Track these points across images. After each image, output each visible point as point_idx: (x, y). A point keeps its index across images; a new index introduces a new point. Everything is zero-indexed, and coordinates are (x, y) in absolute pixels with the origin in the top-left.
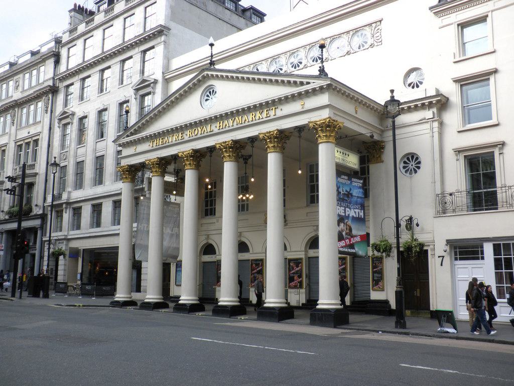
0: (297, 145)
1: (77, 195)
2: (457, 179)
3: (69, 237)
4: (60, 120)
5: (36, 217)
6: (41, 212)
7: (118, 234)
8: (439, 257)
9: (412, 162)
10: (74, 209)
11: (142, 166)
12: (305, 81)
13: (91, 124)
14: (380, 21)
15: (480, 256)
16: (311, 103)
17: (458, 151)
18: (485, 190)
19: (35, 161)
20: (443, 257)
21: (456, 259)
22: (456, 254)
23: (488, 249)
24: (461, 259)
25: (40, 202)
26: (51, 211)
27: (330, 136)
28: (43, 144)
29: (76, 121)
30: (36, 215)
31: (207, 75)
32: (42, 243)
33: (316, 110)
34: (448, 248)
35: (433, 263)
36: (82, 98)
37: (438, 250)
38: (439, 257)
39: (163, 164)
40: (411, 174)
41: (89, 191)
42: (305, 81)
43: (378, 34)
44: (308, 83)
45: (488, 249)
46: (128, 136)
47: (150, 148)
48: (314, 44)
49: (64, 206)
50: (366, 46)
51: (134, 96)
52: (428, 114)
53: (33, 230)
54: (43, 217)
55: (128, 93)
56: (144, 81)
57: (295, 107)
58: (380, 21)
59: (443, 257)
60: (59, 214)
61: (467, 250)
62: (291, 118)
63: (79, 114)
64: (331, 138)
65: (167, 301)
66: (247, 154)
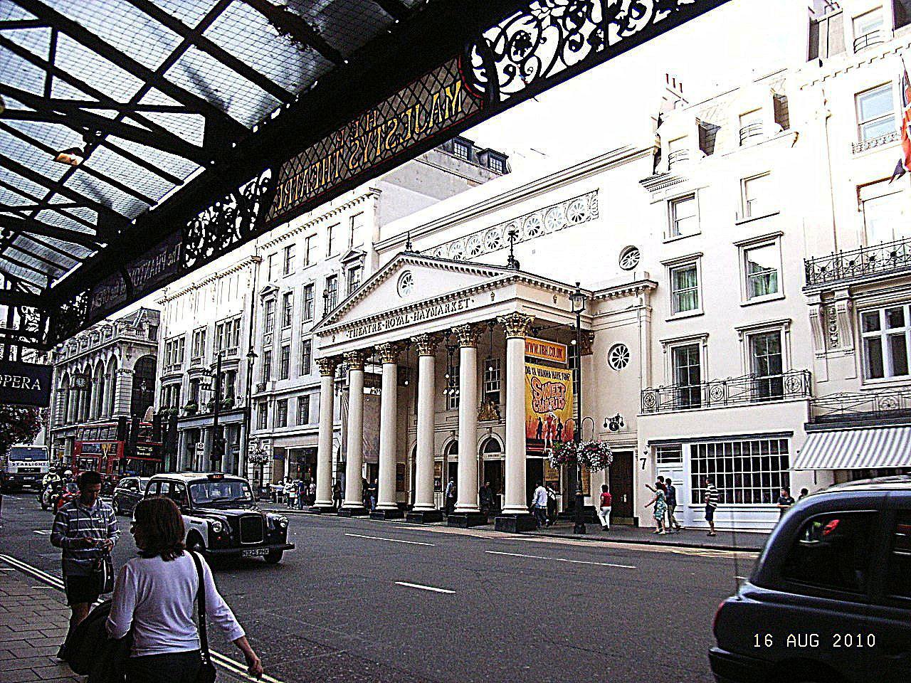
0: (488, 339)
1: (282, 385)
2: (664, 374)
3: (274, 435)
4: (263, 296)
5: (239, 411)
6: (244, 405)
7: (317, 434)
8: (641, 459)
9: (620, 354)
10: (280, 402)
11: (339, 359)
12: (494, 271)
13: (297, 301)
14: (597, 191)
15: (661, 459)
16: (501, 294)
17: (666, 343)
18: (773, 377)
19: (237, 345)
20: (645, 459)
21: (659, 462)
22: (659, 457)
23: (686, 449)
24: (664, 461)
25: (243, 394)
26: (255, 404)
27: (518, 331)
28: (245, 325)
29: (280, 297)
30: (238, 409)
31: (403, 259)
32: (247, 441)
33: (505, 303)
34: (649, 450)
35: (637, 464)
36: (287, 270)
37: (642, 450)
38: (641, 459)
39: (363, 356)
40: (620, 367)
41: (295, 381)
42: (494, 271)
43: (595, 205)
44: (496, 274)
45: (686, 449)
46: (325, 325)
47: (348, 339)
48: (530, 215)
49: (269, 399)
50: (583, 218)
51: (342, 271)
52: (635, 300)
53: (234, 427)
54: (247, 412)
55: (336, 266)
56: (352, 252)
57: (485, 299)
58: (597, 191)
59: (645, 459)
60: (264, 408)
61: (667, 451)
62: (480, 310)
63: (284, 290)
64: (519, 333)
65: (403, 510)
66: (443, 347)
